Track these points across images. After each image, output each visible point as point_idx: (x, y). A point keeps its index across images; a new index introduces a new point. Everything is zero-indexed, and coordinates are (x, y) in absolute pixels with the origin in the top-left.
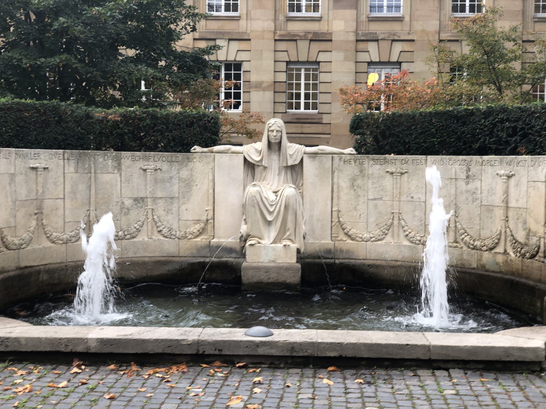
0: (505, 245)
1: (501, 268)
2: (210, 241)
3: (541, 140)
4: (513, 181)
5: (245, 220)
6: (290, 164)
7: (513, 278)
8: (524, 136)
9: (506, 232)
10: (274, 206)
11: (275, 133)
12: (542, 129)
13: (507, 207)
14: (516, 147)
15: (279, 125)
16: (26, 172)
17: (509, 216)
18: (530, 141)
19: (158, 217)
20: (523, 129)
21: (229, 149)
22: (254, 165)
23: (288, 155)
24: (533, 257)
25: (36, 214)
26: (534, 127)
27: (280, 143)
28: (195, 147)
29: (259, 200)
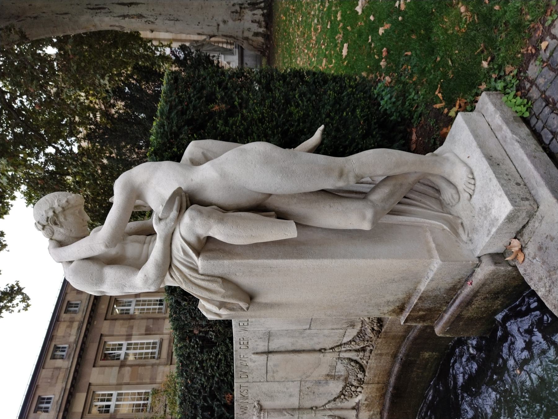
0: (346, 409)
1: (376, 413)
3: (217, 375)
4: (266, 404)
7: (389, 395)
8: (213, 397)
9: (330, 409)
12: (205, 375)
13: (299, 409)
14: (225, 405)
17: (310, 406)
18: (219, 389)
20: (205, 399)
24: (362, 369)
26: (202, 385)
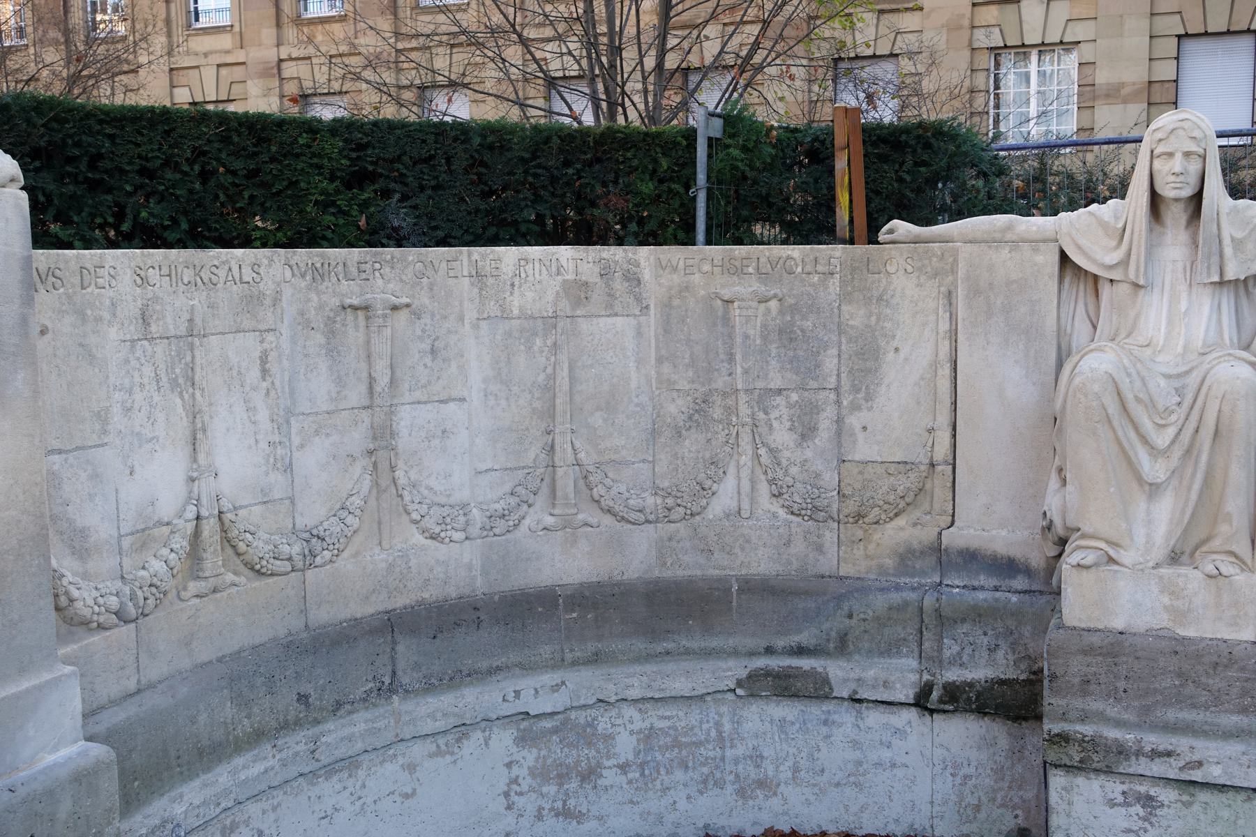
2: (940, 534)
5: (1060, 470)
6: (1230, 275)
10: (1171, 431)
11: (1177, 164)
15: (1197, 134)
16: (330, 321)
19: (771, 450)
21: (1009, 227)
22: (1096, 278)
23: (1227, 241)
25: (371, 453)
27: (1197, 198)
28: (896, 222)
29: (1113, 408)
